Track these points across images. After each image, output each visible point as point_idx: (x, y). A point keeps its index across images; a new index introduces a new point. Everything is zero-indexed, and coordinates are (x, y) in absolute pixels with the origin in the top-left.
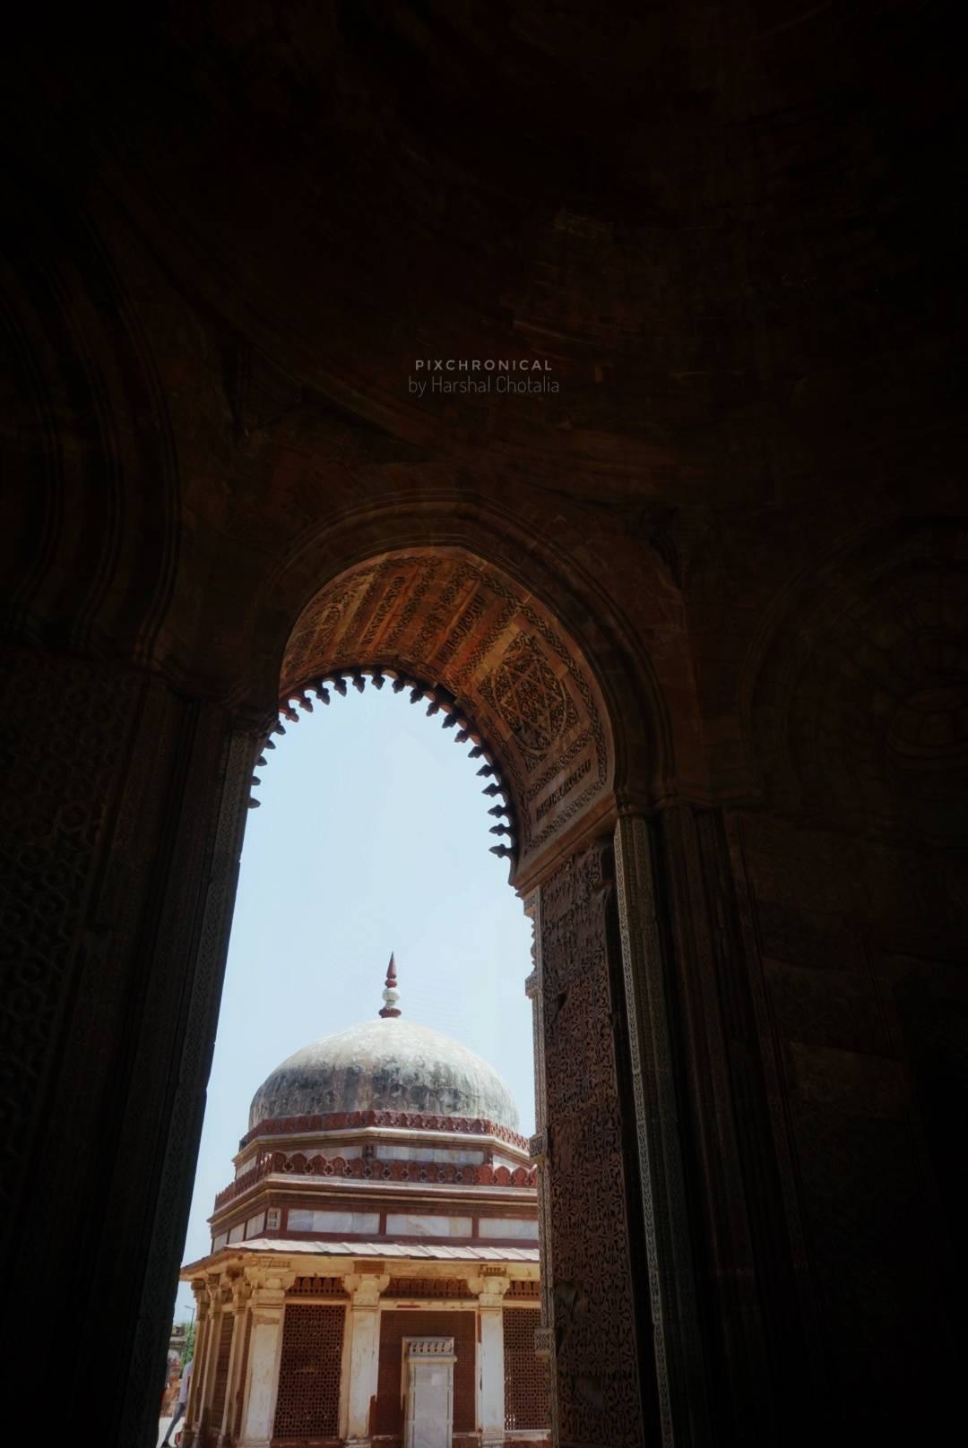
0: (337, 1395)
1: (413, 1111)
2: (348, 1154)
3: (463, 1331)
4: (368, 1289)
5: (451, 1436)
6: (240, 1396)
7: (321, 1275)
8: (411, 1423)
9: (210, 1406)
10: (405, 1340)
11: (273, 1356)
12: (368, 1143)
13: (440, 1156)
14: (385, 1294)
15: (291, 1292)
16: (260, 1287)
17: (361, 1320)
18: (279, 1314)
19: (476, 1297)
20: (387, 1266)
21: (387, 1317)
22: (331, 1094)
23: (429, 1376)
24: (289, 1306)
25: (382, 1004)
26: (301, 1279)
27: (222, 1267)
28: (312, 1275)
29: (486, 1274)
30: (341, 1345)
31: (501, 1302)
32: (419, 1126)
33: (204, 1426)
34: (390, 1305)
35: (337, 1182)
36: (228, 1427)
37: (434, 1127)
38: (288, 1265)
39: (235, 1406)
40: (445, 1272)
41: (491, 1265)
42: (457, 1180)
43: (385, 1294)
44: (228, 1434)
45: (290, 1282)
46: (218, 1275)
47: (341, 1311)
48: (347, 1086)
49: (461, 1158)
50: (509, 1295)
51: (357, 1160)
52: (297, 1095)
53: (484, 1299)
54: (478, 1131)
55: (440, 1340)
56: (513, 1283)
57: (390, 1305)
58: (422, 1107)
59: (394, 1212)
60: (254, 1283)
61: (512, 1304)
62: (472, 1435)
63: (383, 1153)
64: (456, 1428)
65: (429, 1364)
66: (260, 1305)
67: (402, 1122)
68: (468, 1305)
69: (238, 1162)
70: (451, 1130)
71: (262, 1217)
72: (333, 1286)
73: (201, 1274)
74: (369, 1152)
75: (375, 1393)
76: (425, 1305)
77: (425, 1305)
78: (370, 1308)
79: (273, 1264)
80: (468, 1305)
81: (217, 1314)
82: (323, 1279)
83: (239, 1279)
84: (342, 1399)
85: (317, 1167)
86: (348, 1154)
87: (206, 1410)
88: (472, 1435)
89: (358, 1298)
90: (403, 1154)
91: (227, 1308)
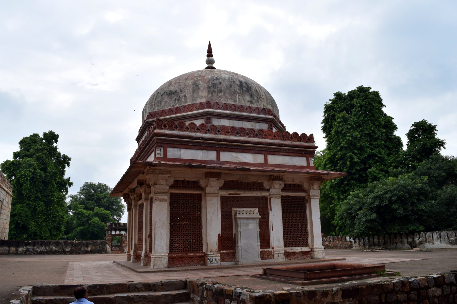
0: (201, 234)
1: (230, 102)
2: (198, 122)
3: (264, 207)
4: (213, 186)
5: (260, 250)
6: (150, 236)
7: (187, 179)
8: (239, 244)
9: (137, 243)
10: (234, 209)
11: (166, 216)
12: (208, 116)
13: (247, 125)
14: (222, 188)
15: (171, 187)
16: (155, 184)
17: (210, 200)
18: (167, 197)
19: (268, 190)
20: (223, 175)
21: (224, 200)
22: (185, 96)
23: (247, 225)
24: (170, 193)
25: (206, 66)
26: (177, 181)
27: (134, 184)
28: (183, 179)
29: (273, 180)
30: (201, 211)
31: (280, 193)
32: (235, 110)
33: (135, 252)
34: (225, 193)
35: (193, 134)
36: (146, 250)
37: (240, 111)
38: (169, 173)
39: (148, 241)
40: (252, 179)
41: (276, 174)
42: (256, 136)
43: (222, 188)
44: (146, 252)
45: (171, 182)
46: (134, 189)
47: (199, 198)
48: (194, 91)
49: (257, 126)
50: (283, 190)
51: (202, 124)
52: (166, 99)
53: (272, 191)
54: (264, 114)
55: (252, 209)
56: (285, 185)
57: (225, 193)
58: (235, 101)
59: (224, 151)
60: (151, 183)
61: (285, 194)
62: (268, 250)
63: (216, 122)
64: (261, 247)
65: (247, 219)
66: (156, 193)
67: (226, 107)
68: (264, 194)
69: (138, 139)
70: (251, 112)
71: (153, 155)
72: (195, 185)
73: (126, 191)
74: (208, 121)
75: (220, 232)
76: (243, 194)
77: (243, 194)
78: (215, 195)
79: (161, 172)
80: (264, 194)
81: (135, 206)
82: (188, 181)
83: (144, 186)
84: (204, 236)
85: (182, 127)
86: (198, 122)
87: (135, 244)
88: (268, 250)
89: (208, 190)
90: (226, 123)
91: (140, 202)
